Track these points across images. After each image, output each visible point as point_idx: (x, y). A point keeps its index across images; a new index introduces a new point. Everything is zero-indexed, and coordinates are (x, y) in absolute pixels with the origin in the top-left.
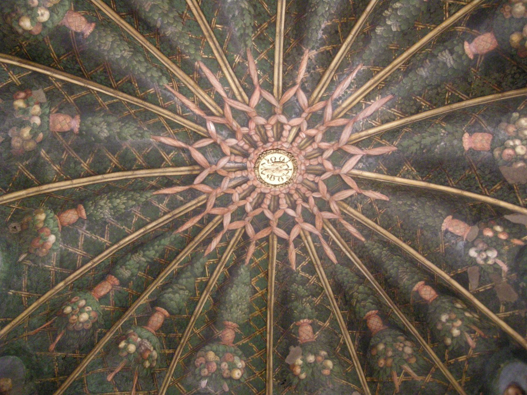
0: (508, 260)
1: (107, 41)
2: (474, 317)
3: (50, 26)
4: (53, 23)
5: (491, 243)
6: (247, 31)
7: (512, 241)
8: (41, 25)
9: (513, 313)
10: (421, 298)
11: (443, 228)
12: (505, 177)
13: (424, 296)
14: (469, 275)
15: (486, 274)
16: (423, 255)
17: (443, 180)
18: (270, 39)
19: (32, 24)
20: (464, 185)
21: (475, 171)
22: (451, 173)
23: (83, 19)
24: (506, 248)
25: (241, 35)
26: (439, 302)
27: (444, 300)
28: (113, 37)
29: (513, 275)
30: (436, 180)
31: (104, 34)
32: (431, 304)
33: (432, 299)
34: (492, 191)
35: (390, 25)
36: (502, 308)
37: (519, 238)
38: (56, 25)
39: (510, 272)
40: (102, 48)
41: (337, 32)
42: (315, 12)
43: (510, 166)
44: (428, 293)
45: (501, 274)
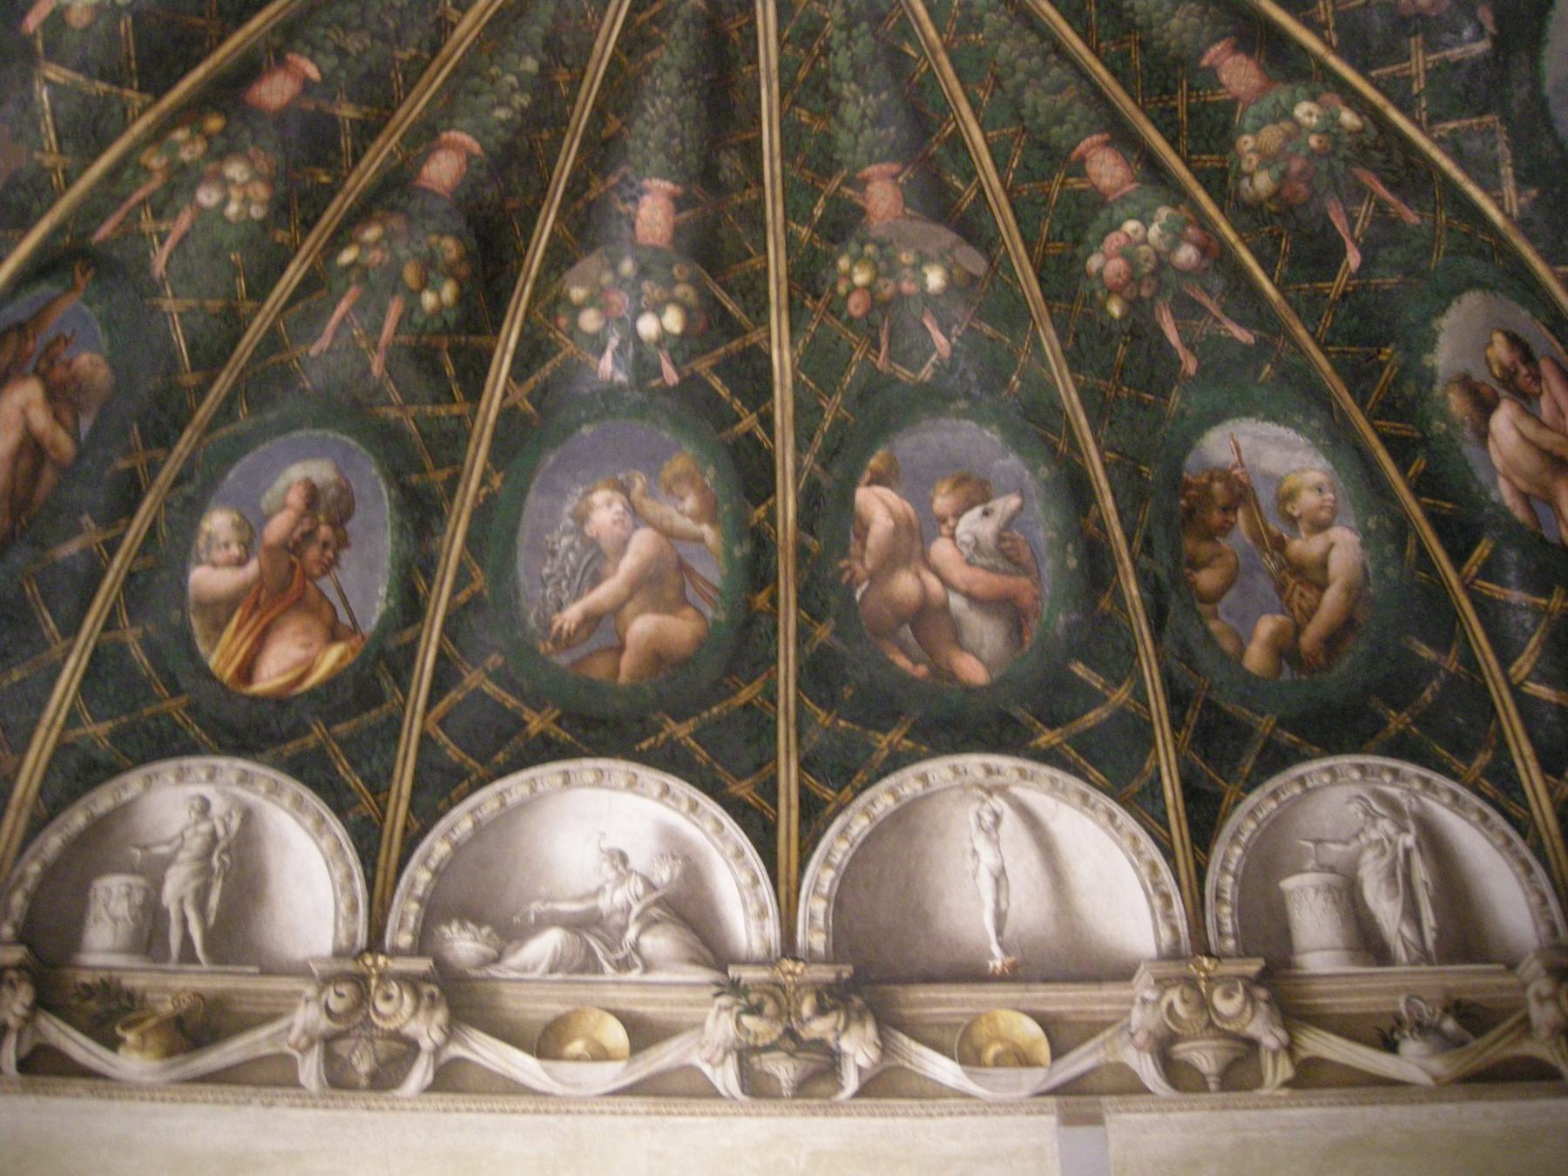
1: (1185, 20)
3: (1300, 91)
4: (1294, 92)
6: (844, 35)
8: (1320, 100)
18: (789, 48)
19: (1339, 112)
23: (1224, 77)
25: (856, 24)
28: (1168, 30)
31: (1188, 37)
35: (505, 72)
38: (1289, 87)
40: (1199, 8)
41: (629, 53)
42: (685, 77)
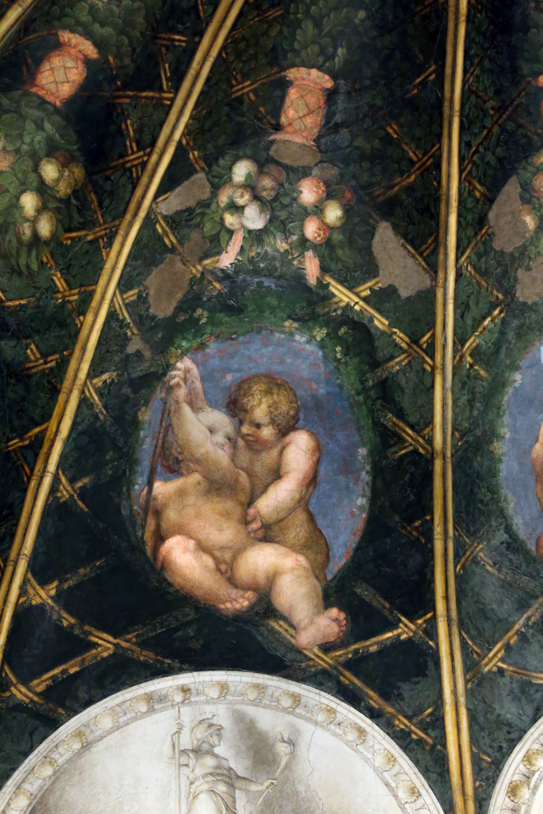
0: (251, 260)
2: (34, 221)
5: (284, 206)
7: (309, 254)
9: (128, 326)
10: (39, 62)
11: (292, 74)
12: (498, 199)
13: (46, 66)
14: (186, 183)
15: (198, 220)
16: (224, 48)
17: (472, 52)
20: (470, 109)
21: (496, 122)
22: (486, 63)
24: (282, 246)
26: (36, 113)
27: (48, 126)
29: (217, 285)
30: (473, 35)
32: (27, 94)
33: (41, 93)
34: (470, 183)
36: (132, 295)
37: (324, 269)
39: (219, 274)
43: (522, 198)
44: (60, 76)
45: (206, 256)
